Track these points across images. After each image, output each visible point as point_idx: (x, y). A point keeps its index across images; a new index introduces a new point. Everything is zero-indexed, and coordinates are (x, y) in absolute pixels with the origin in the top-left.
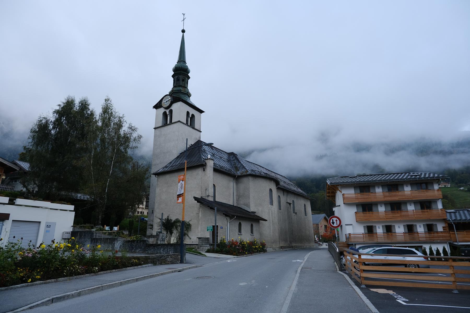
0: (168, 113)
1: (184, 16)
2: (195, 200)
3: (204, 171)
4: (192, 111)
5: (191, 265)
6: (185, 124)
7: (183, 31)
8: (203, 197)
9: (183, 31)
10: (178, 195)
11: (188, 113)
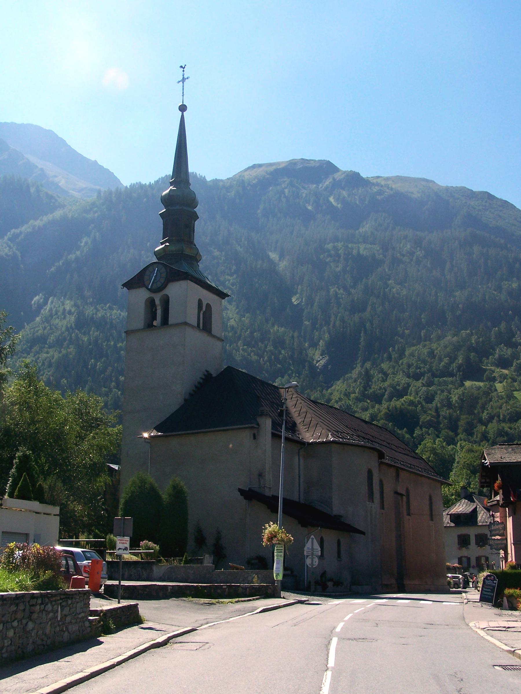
0: (157, 302)
1: (183, 71)
2: (241, 495)
3: (255, 437)
4: (208, 297)
5: (288, 600)
6: (193, 327)
7: (183, 108)
8: (252, 489)
9: (183, 108)
10: (488, 557)
11: (200, 302)
